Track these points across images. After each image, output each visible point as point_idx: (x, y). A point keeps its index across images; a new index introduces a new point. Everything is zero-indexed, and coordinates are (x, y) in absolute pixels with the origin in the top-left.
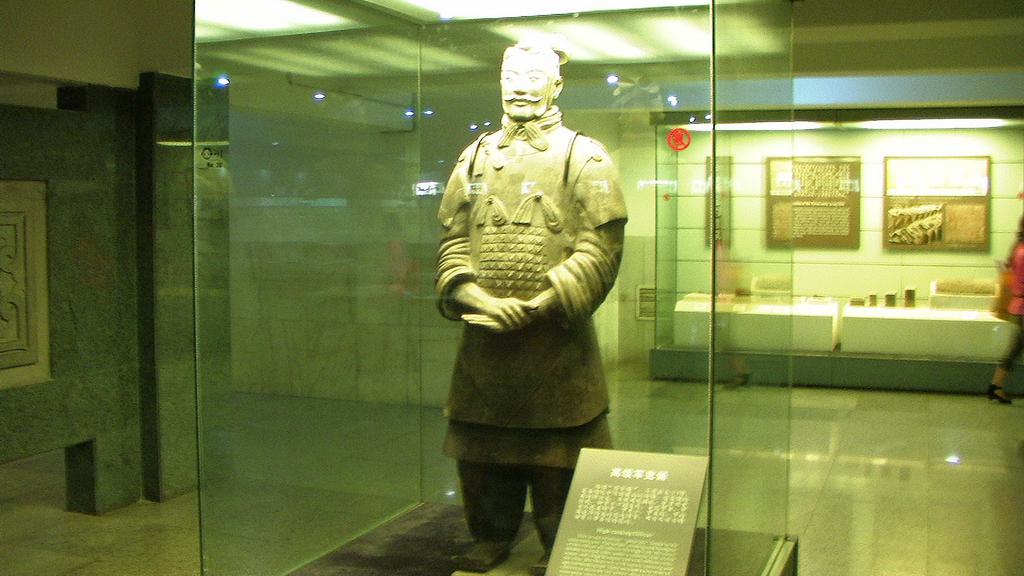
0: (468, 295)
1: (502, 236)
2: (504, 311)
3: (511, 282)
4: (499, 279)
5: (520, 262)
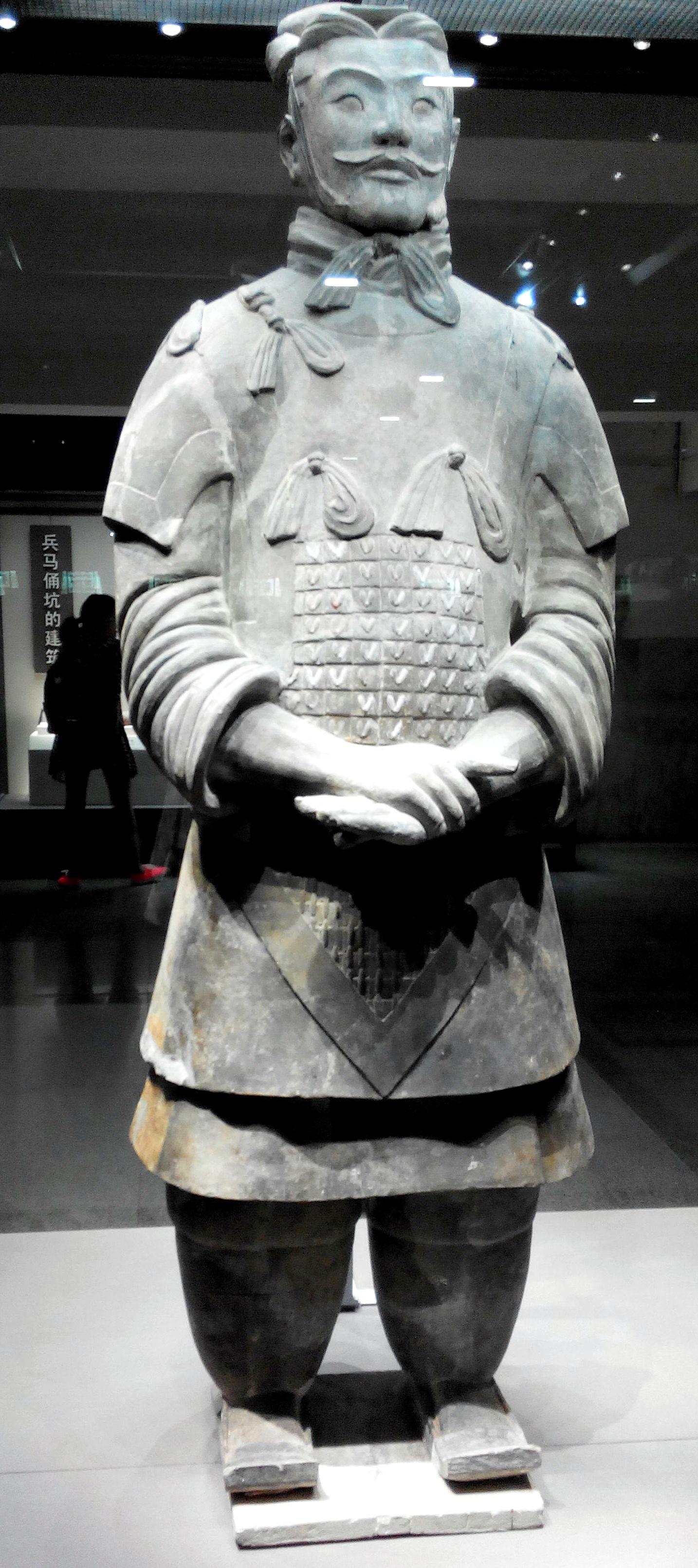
1: (367, 568)
2: (422, 783)
3: (402, 698)
4: (366, 690)
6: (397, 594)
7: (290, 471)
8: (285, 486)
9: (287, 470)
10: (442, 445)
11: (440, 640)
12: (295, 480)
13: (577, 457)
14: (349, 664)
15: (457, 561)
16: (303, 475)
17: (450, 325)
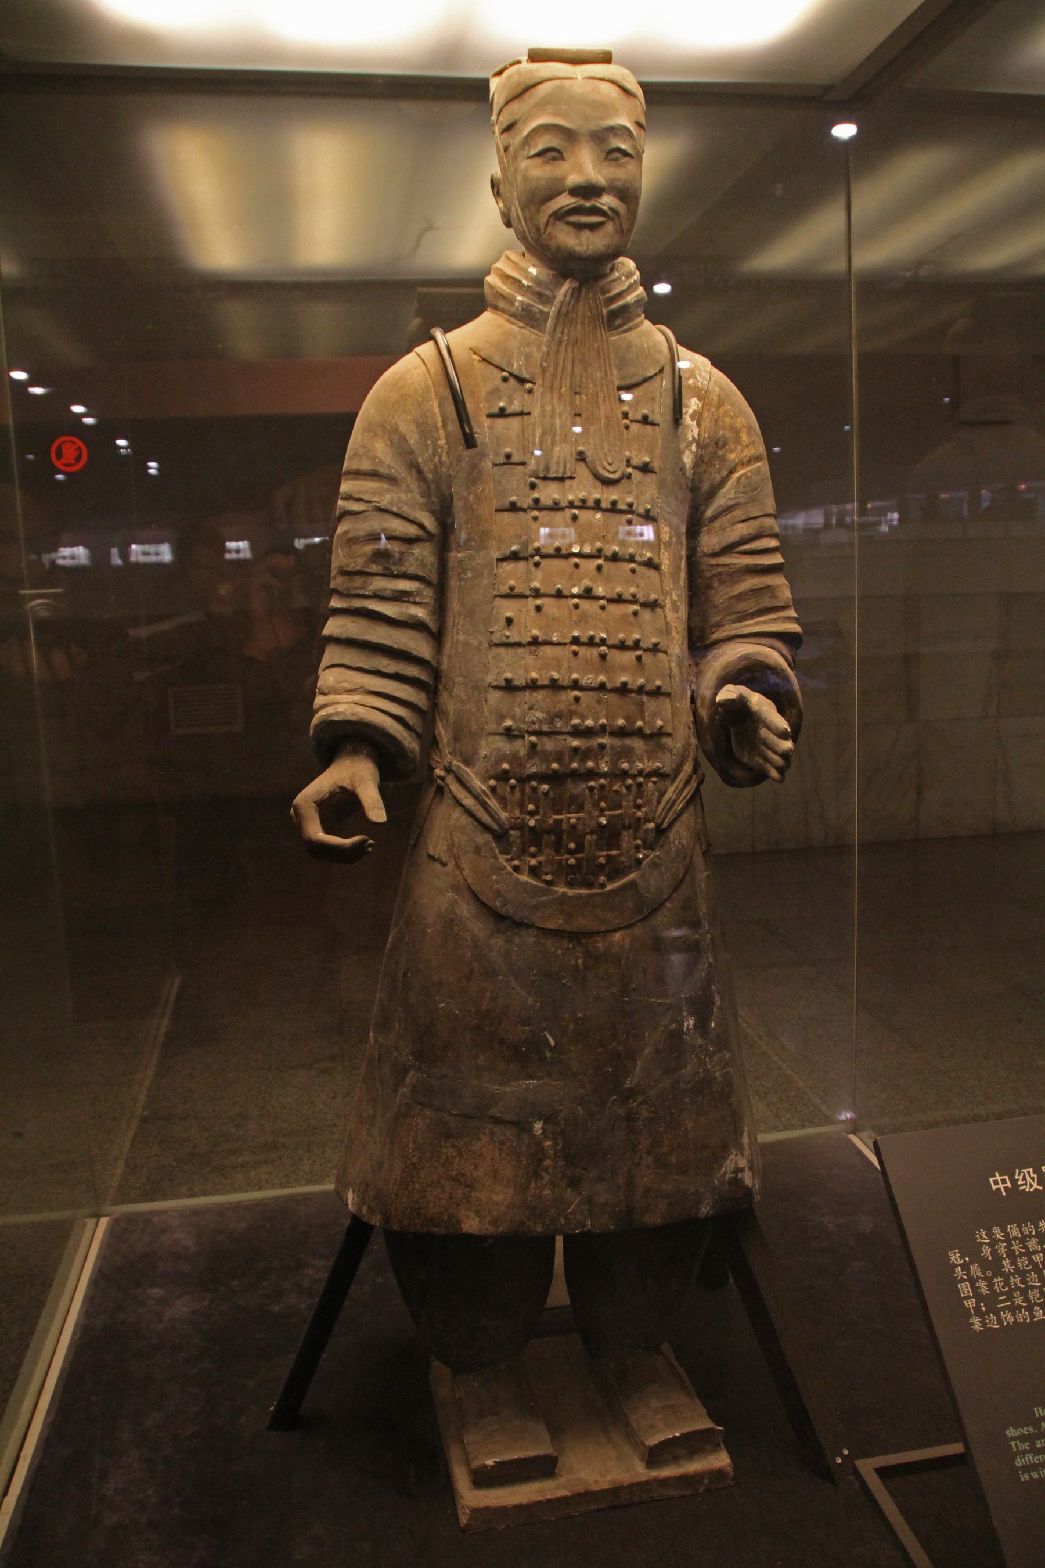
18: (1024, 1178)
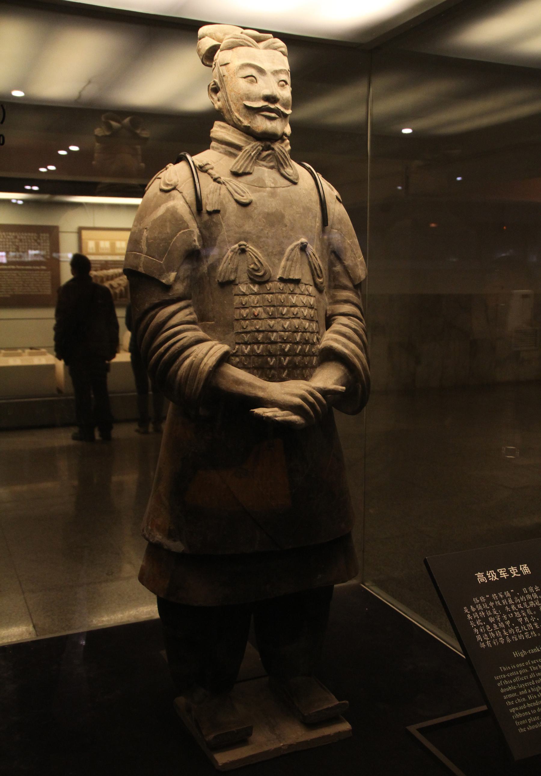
0: (238, 382)
1: (269, 297)
4: (271, 355)
5: (296, 331)
6: (284, 310)
7: (229, 251)
8: (228, 257)
9: (228, 250)
10: (298, 239)
11: (302, 330)
12: (233, 254)
13: (349, 244)
14: (263, 343)
15: (307, 293)
16: (237, 252)
17: (295, 184)
18: (491, 575)
